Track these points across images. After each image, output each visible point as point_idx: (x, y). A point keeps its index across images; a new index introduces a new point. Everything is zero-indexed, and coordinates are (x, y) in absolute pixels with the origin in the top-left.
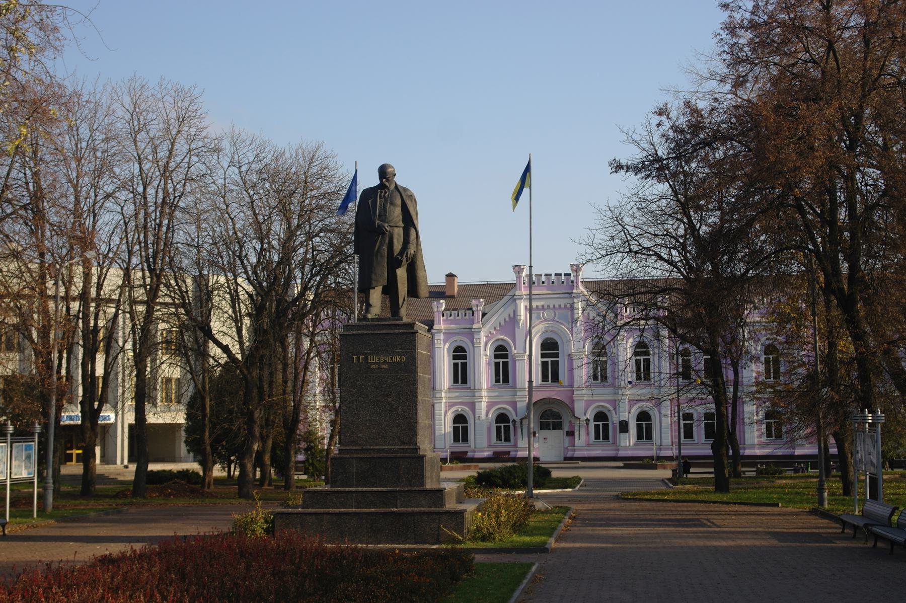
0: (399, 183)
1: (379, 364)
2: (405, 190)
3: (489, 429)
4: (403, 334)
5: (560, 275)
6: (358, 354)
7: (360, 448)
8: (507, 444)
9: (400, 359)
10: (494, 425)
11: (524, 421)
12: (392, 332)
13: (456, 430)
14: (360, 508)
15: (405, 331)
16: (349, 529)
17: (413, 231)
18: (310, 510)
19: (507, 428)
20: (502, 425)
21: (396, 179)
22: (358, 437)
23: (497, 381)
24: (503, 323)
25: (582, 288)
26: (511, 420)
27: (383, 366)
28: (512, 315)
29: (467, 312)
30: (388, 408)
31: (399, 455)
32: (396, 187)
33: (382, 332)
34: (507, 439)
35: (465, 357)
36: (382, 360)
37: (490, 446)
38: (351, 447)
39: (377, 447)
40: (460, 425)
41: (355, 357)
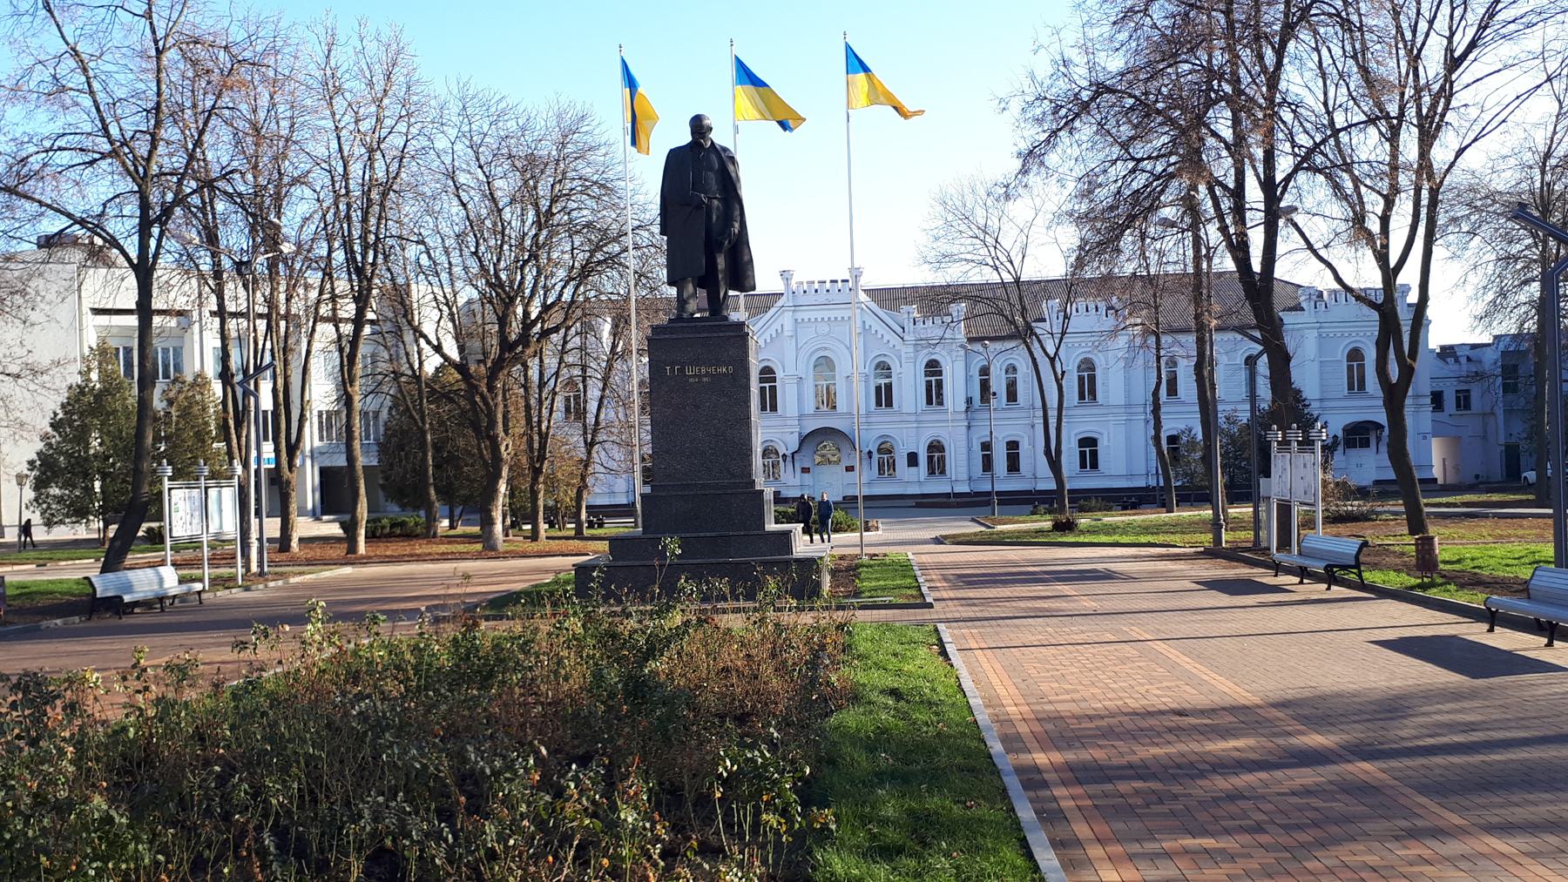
0: (715, 141)
1: (700, 376)
2: (725, 149)
5: (836, 281)
6: (672, 365)
11: (796, 456)
18: (620, 563)
21: (713, 135)
25: (863, 297)
27: (705, 379)
30: (713, 432)
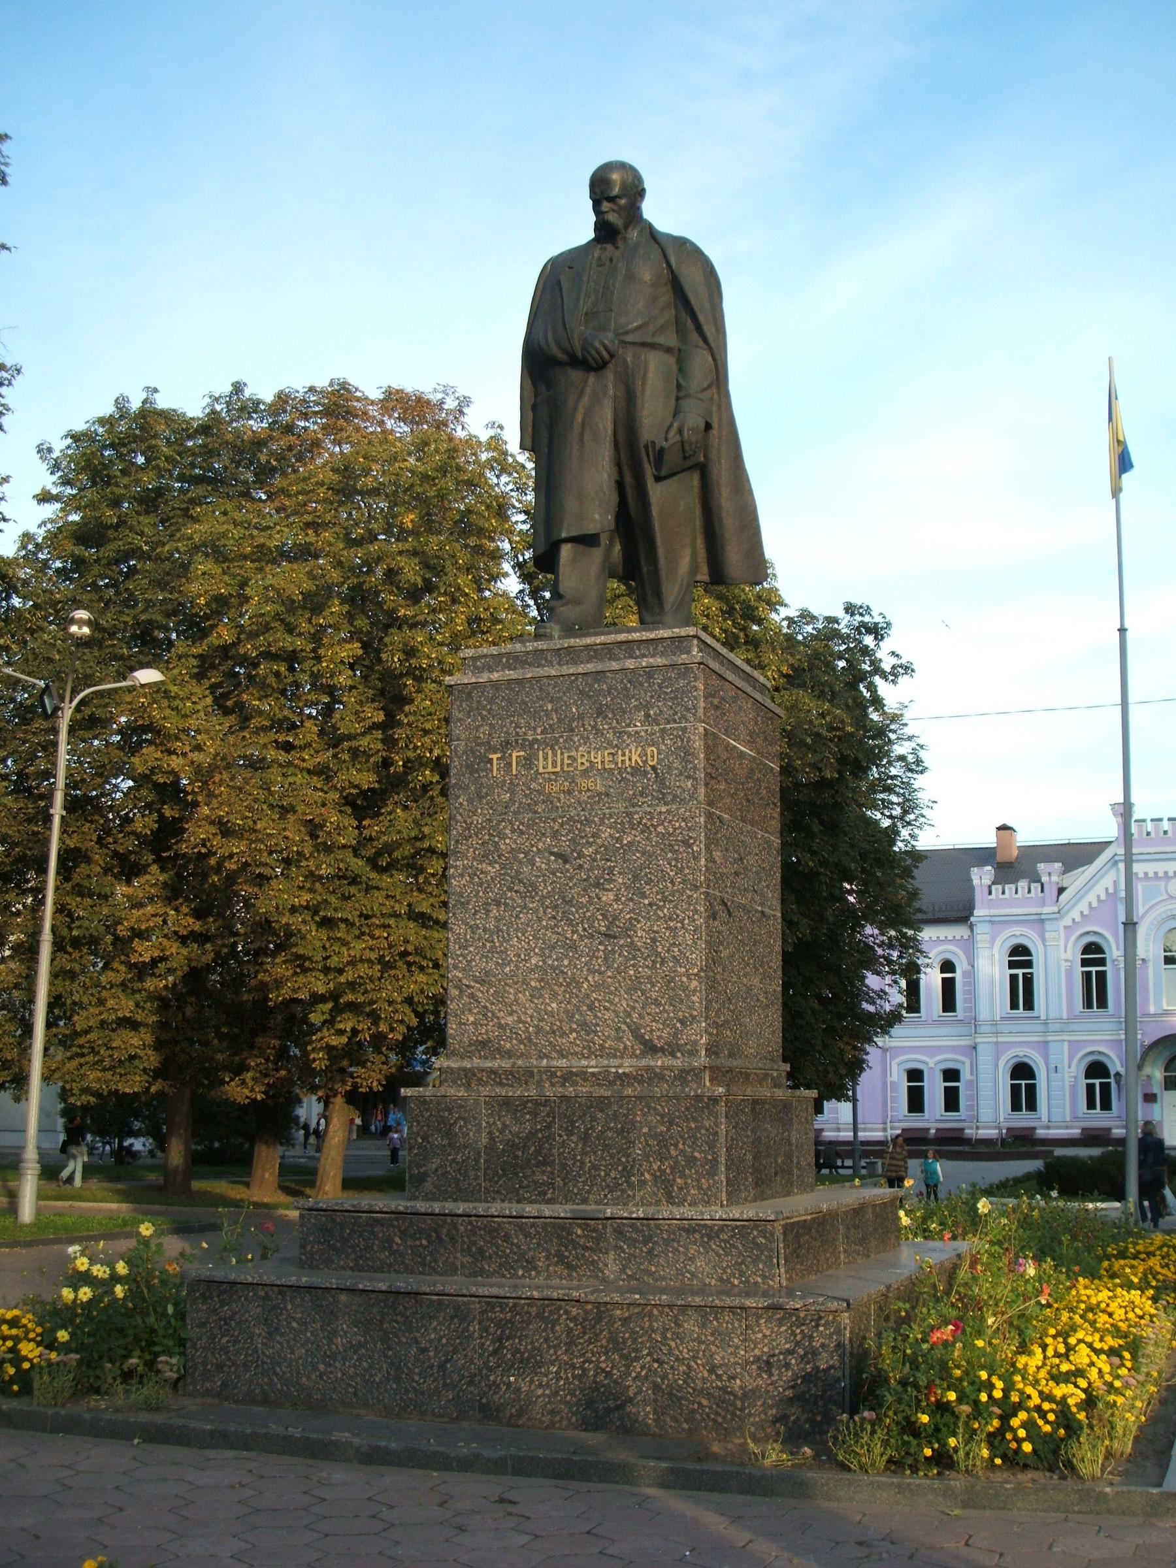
3: (1073, 1088)
4: (650, 671)
6: (506, 745)
7: (506, 1064)
8: (1106, 1114)
9: (643, 754)
10: (1084, 1082)
12: (615, 665)
13: (1015, 1090)
14: (481, 1272)
15: (659, 661)
16: (424, 1350)
17: (700, 360)
19: (1105, 1088)
20: (1097, 1082)
22: (500, 1026)
23: (1088, 1005)
24: (1095, 904)
26: (1112, 1073)
28: (1111, 890)
29: (1033, 886)
31: (629, 1091)
32: (652, 233)
33: (581, 669)
34: (1106, 1105)
35: (1029, 964)
36: (582, 762)
37: (1075, 1118)
38: (476, 1062)
39: (563, 1063)
40: (1023, 1082)
41: (494, 757)
